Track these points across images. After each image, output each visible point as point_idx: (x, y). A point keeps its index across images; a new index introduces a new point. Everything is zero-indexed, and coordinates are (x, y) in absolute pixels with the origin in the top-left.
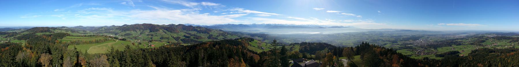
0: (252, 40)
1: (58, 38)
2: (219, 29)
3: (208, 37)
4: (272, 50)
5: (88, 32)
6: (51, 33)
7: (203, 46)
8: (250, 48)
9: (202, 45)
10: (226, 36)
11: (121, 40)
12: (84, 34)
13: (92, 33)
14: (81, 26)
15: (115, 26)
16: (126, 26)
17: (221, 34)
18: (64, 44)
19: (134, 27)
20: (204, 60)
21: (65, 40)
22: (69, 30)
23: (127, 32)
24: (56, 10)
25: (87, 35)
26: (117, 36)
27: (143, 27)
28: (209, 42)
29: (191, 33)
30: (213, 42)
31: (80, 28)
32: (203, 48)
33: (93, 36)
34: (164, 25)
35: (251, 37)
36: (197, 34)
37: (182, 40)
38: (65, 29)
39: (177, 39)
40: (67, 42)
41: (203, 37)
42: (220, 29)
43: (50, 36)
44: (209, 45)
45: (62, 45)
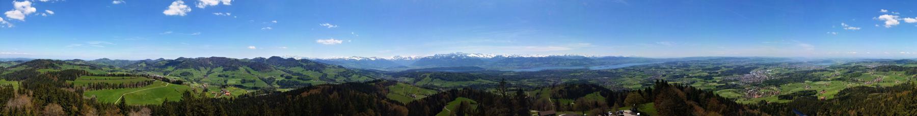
0: (394, 83)
3: (319, 78)
4: (427, 97)
5: (117, 68)
8: (390, 96)
10: (349, 76)
11: (174, 83)
12: (111, 71)
13: (124, 70)
14: (106, 59)
15: (165, 60)
16: (182, 61)
17: (341, 73)
19: (195, 63)
21: (79, 82)
23: (184, 70)
25: (117, 73)
26: (167, 77)
27: (210, 63)
31: (104, 62)
33: (128, 75)
34: (246, 59)
35: (393, 79)
37: (278, 83)
39: (270, 81)
42: (340, 65)
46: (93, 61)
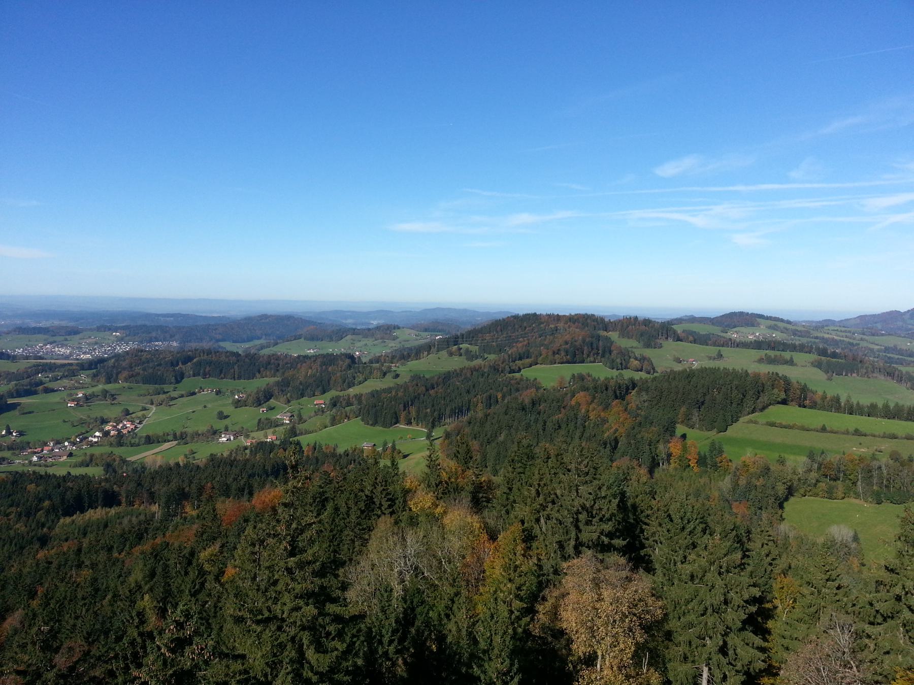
1: (687, 421)
6: (628, 374)
18: (743, 482)
22: (794, 348)
24: (669, 170)
38: (755, 334)
40: (782, 462)
43: (622, 392)
45: (726, 483)
46: (844, 325)
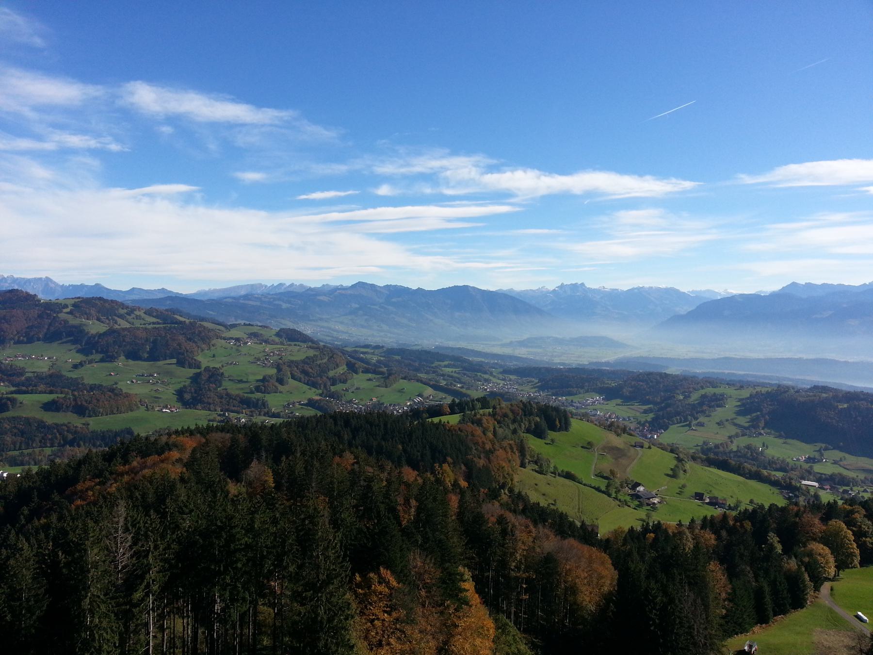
2: (276, 325)
3: (180, 393)
7: (134, 472)
9: (126, 461)
10: (334, 382)
17: (291, 364)
20: (138, 595)
28: (190, 432)
29: (20, 362)
30: (222, 430)
32: (131, 488)
35: (542, 397)
36: (75, 367)
41: (139, 390)
42: (289, 324)
44: (186, 456)
